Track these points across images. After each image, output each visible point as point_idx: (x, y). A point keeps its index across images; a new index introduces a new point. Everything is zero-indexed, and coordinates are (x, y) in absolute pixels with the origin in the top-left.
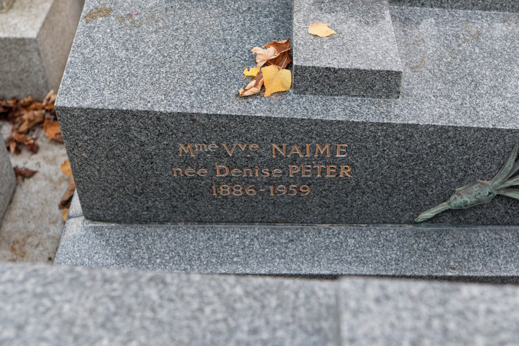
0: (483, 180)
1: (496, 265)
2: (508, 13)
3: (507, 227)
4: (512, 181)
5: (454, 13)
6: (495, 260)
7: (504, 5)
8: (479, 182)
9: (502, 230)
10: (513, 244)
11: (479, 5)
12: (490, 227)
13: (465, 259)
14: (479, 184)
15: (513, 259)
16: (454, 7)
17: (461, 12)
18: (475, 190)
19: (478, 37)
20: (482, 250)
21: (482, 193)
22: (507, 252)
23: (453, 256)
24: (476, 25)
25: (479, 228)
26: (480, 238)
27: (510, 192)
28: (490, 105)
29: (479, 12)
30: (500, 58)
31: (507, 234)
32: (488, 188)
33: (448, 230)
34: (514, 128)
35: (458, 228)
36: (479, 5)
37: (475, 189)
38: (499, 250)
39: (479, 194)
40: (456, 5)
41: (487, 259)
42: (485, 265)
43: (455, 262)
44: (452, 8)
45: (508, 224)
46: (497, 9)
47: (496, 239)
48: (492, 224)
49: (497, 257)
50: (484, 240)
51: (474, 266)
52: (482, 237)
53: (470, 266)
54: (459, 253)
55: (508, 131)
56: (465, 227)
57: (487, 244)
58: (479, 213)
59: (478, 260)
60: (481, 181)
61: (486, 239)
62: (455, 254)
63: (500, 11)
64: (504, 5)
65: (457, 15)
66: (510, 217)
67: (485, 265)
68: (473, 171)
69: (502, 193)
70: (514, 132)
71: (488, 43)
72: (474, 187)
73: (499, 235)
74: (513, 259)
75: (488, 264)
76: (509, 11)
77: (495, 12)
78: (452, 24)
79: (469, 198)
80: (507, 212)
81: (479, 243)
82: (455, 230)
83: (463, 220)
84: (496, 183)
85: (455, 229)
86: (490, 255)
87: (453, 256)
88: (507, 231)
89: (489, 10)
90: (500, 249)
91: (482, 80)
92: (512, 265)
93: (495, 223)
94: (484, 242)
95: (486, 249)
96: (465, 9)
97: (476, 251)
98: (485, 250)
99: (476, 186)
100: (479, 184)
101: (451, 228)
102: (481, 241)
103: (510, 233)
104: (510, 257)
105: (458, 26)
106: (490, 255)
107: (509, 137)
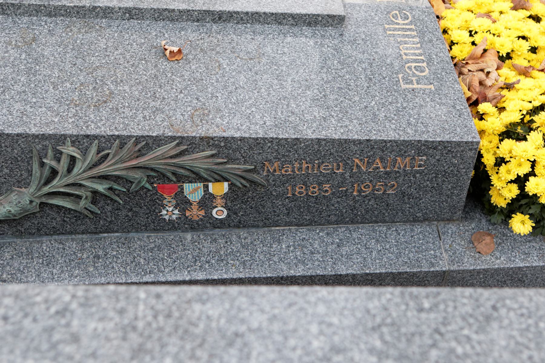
0: (21, 188)
1: (50, 275)
2: (75, 19)
3: (73, 236)
4: (48, 188)
5: (18, 20)
6: (51, 270)
7: (68, 11)
8: (16, 190)
9: (68, 239)
10: (74, 253)
11: (43, 11)
12: (56, 237)
13: (20, 270)
14: (16, 192)
15: (69, 268)
16: (18, 14)
17: (25, 19)
18: (14, 198)
19: (31, 43)
20: (41, 260)
21: (22, 201)
22: (65, 261)
23: (8, 268)
24: (36, 31)
25: (44, 239)
26: (43, 249)
27: (52, 199)
28: (8, 111)
29: (45, 18)
30: (44, 63)
31: (71, 243)
32: (25, 195)
33: (12, 242)
34: (23, 131)
35: (23, 240)
36: (43, 11)
37: (13, 197)
38: (58, 259)
39: (20, 202)
40: (19, 11)
41: (43, 270)
42: (39, 276)
43: (9, 274)
44: (16, 15)
45: (71, 233)
46: (63, 16)
47: (58, 249)
48: (55, 233)
49: (54, 267)
50: (46, 250)
51: (26, 277)
52: (45, 248)
53: (23, 277)
54: (16, 264)
55: (18, 135)
56: (29, 238)
57: (47, 254)
58: (36, 222)
59: (33, 271)
60: (17, 189)
61: (48, 250)
62: (11, 267)
63: (67, 17)
64: (68, 11)
65: (20, 22)
66: (70, 225)
67: (39, 276)
68: (5, 178)
69: (44, 200)
70: (24, 136)
71: (39, 49)
72: (12, 196)
73: (63, 244)
74: (69, 268)
75: (42, 275)
76: (75, 17)
77: (62, 18)
78: (10, 31)
79: (11, 207)
80: (64, 221)
81: (39, 253)
82: (18, 242)
83: (23, 231)
84: (32, 190)
85: (18, 241)
86: (47, 265)
87: (8, 268)
88: (73, 240)
89: (55, 16)
90: (59, 259)
91: (13, 86)
92: (67, 274)
93: (58, 232)
94: (45, 252)
95: (45, 259)
96: (30, 15)
97: (34, 262)
98: (43, 260)
99: (14, 194)
100: (16, 192)
101: (15, 240)
102: (43, 251)
103: (75, 242)
104: (67, 267)
105: (15, 33)
106: (47, 265)
107: (22, 142)
